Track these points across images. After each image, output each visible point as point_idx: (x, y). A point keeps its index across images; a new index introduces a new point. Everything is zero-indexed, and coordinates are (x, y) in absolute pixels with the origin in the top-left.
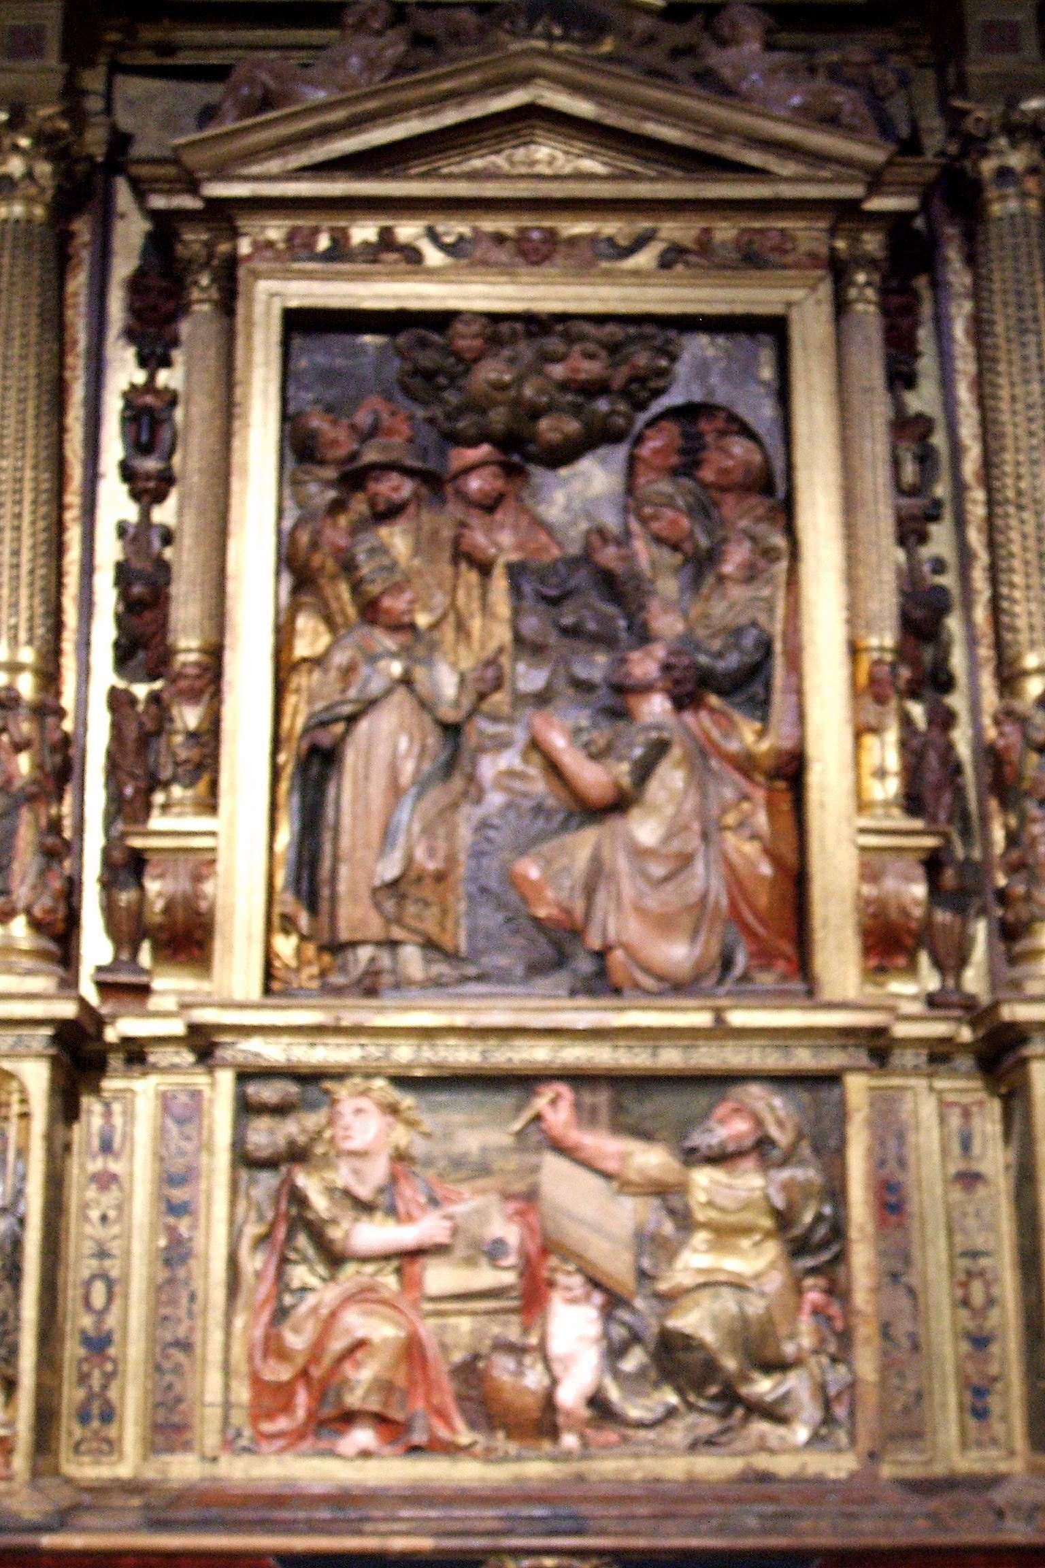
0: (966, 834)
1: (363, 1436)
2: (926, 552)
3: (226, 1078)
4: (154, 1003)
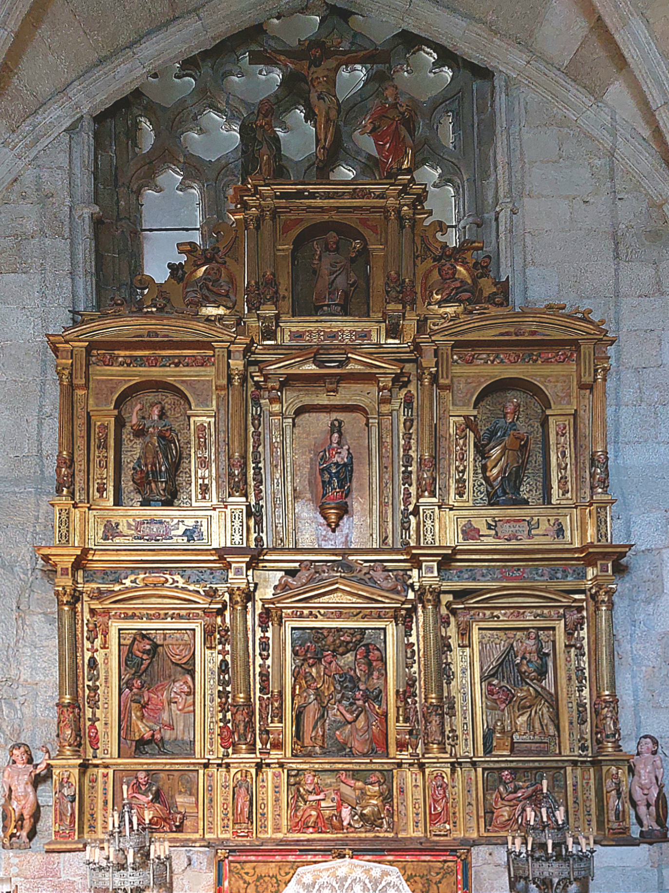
0: (418, 723)
1: (311, 830)
2: (413, 670)
3: (285, 771)
4: (271, 757)
